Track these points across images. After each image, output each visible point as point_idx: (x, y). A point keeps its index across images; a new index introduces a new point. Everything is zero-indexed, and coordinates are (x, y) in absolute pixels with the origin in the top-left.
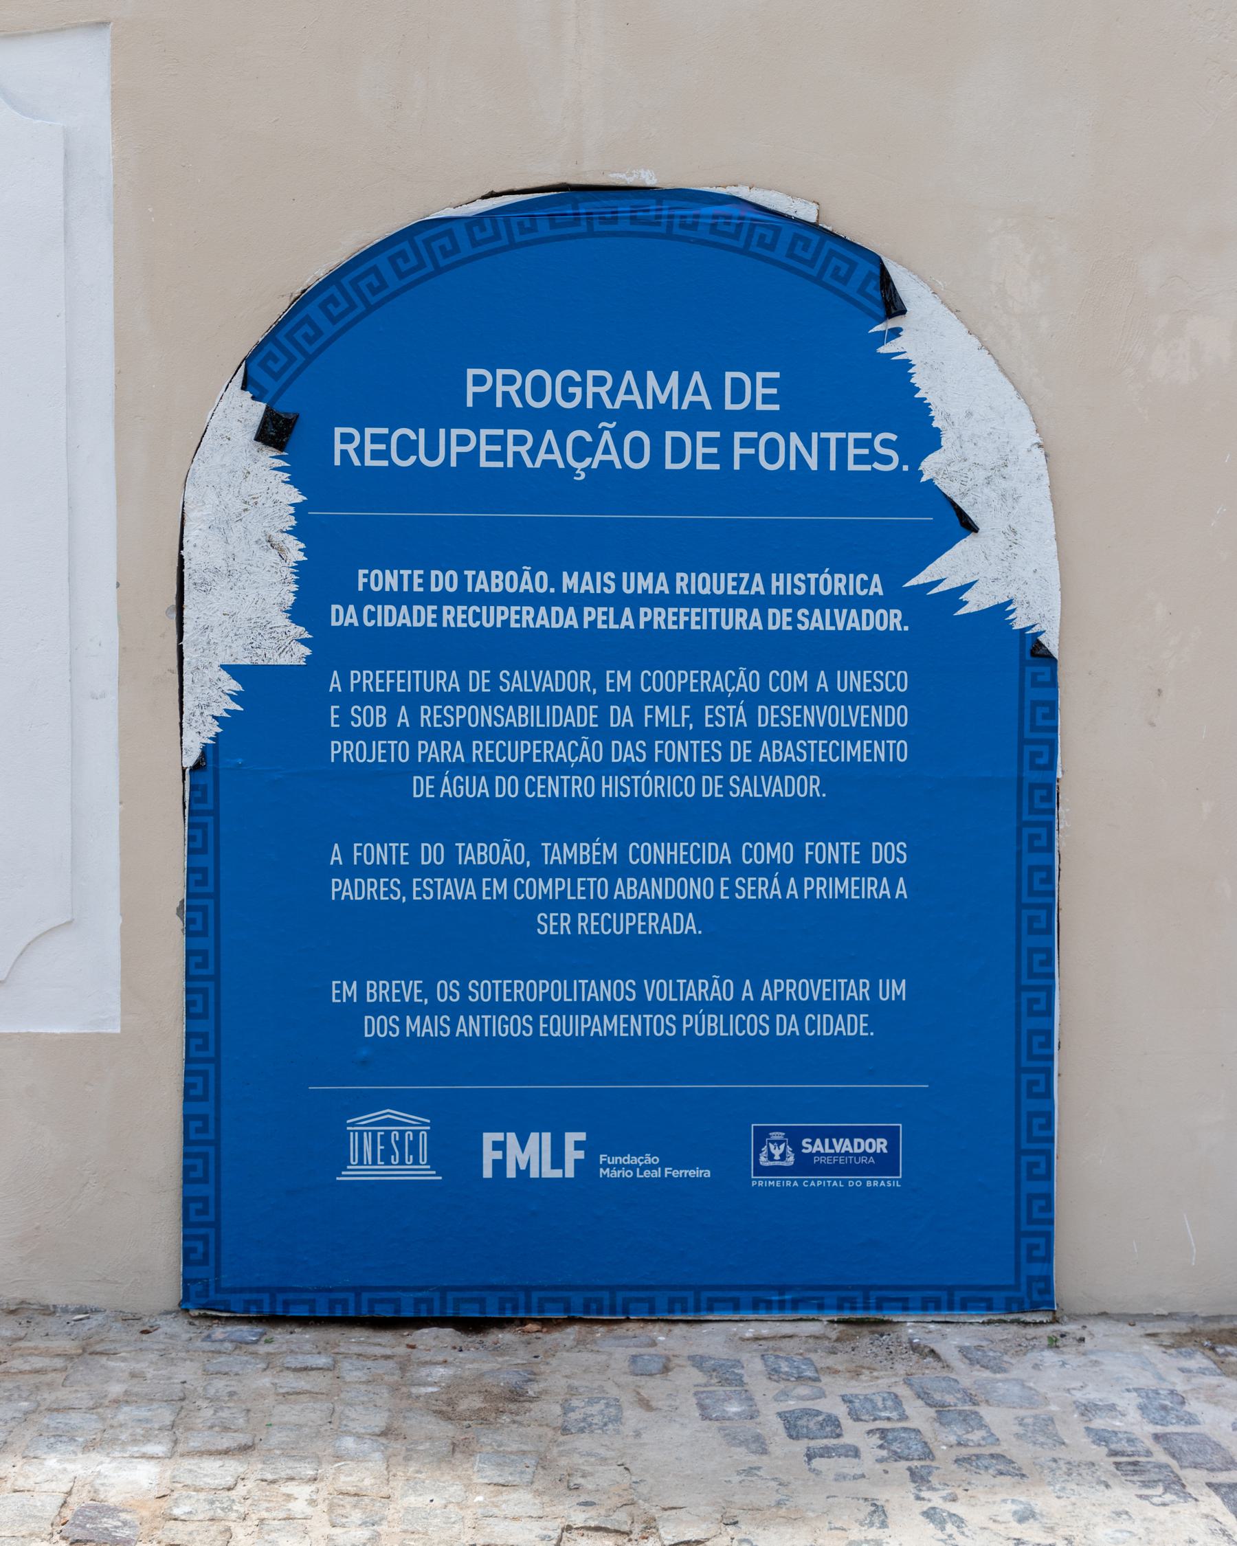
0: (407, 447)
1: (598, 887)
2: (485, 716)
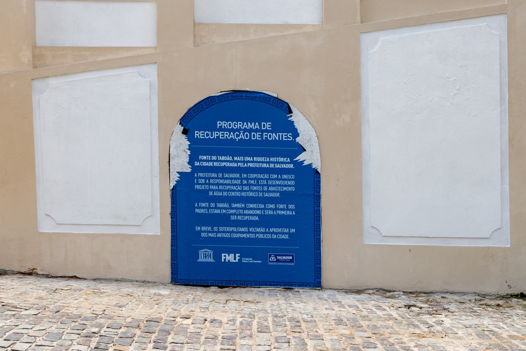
0: (208, 135)
1: (241, 211)
2: (221, 181)
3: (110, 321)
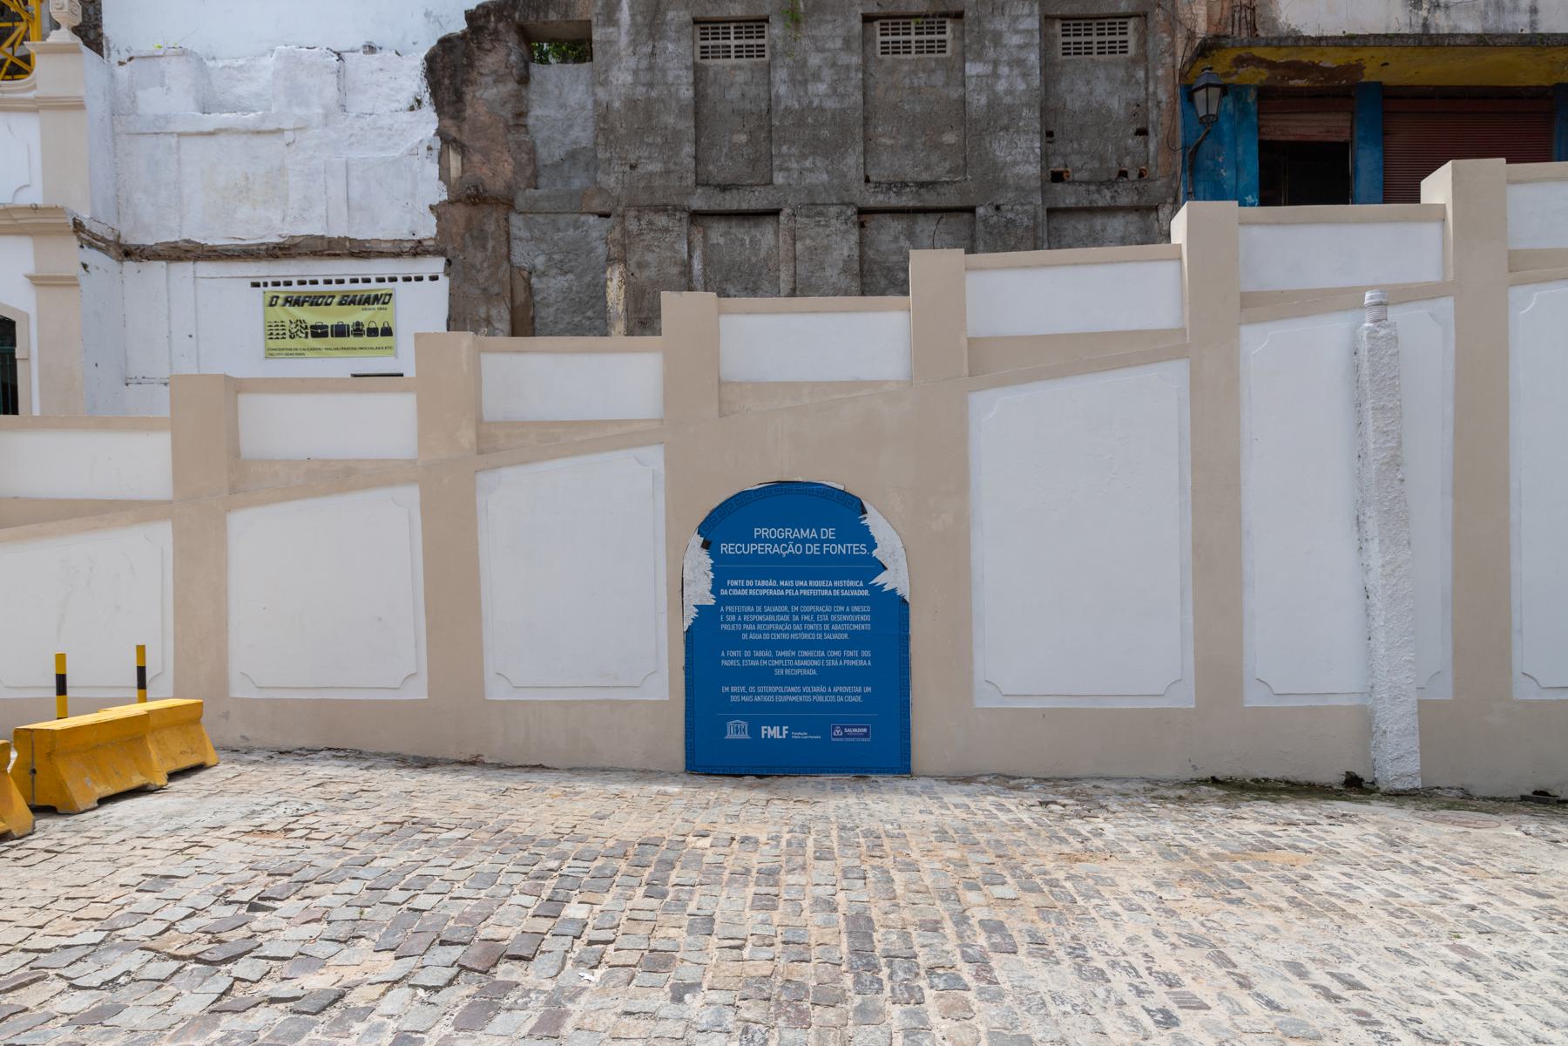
1: (790, 662)
2: (761, 618)
3: (581, 846)
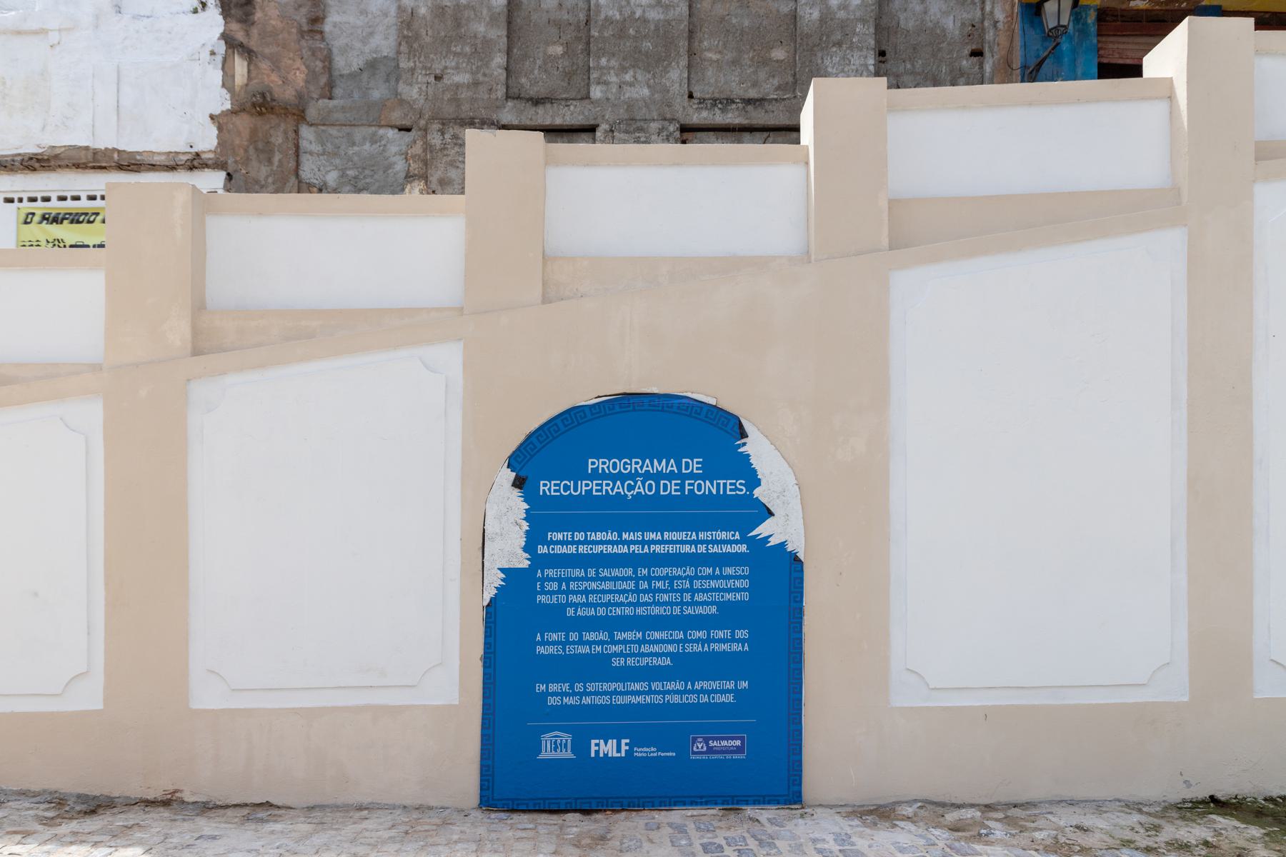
0: (567, 488)
2: (594, 585)
